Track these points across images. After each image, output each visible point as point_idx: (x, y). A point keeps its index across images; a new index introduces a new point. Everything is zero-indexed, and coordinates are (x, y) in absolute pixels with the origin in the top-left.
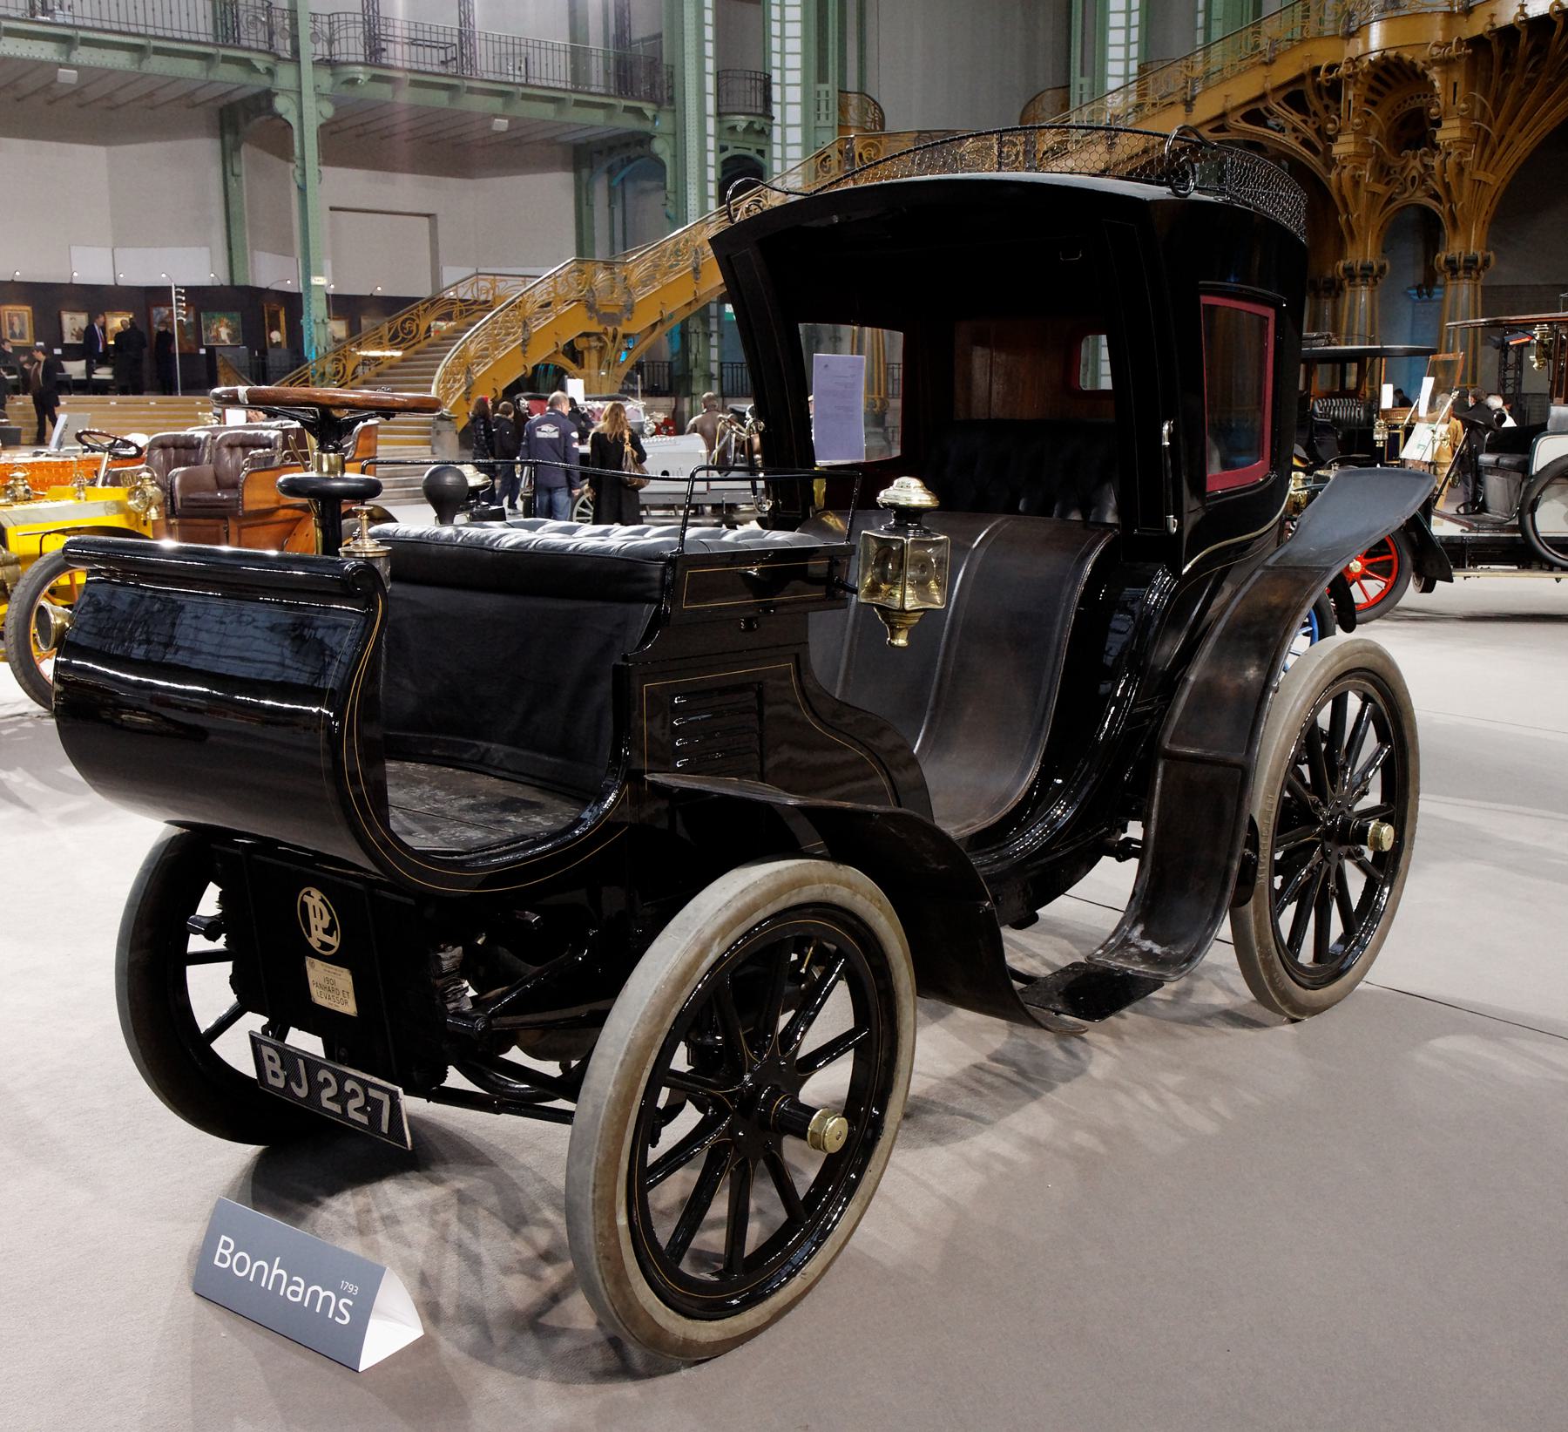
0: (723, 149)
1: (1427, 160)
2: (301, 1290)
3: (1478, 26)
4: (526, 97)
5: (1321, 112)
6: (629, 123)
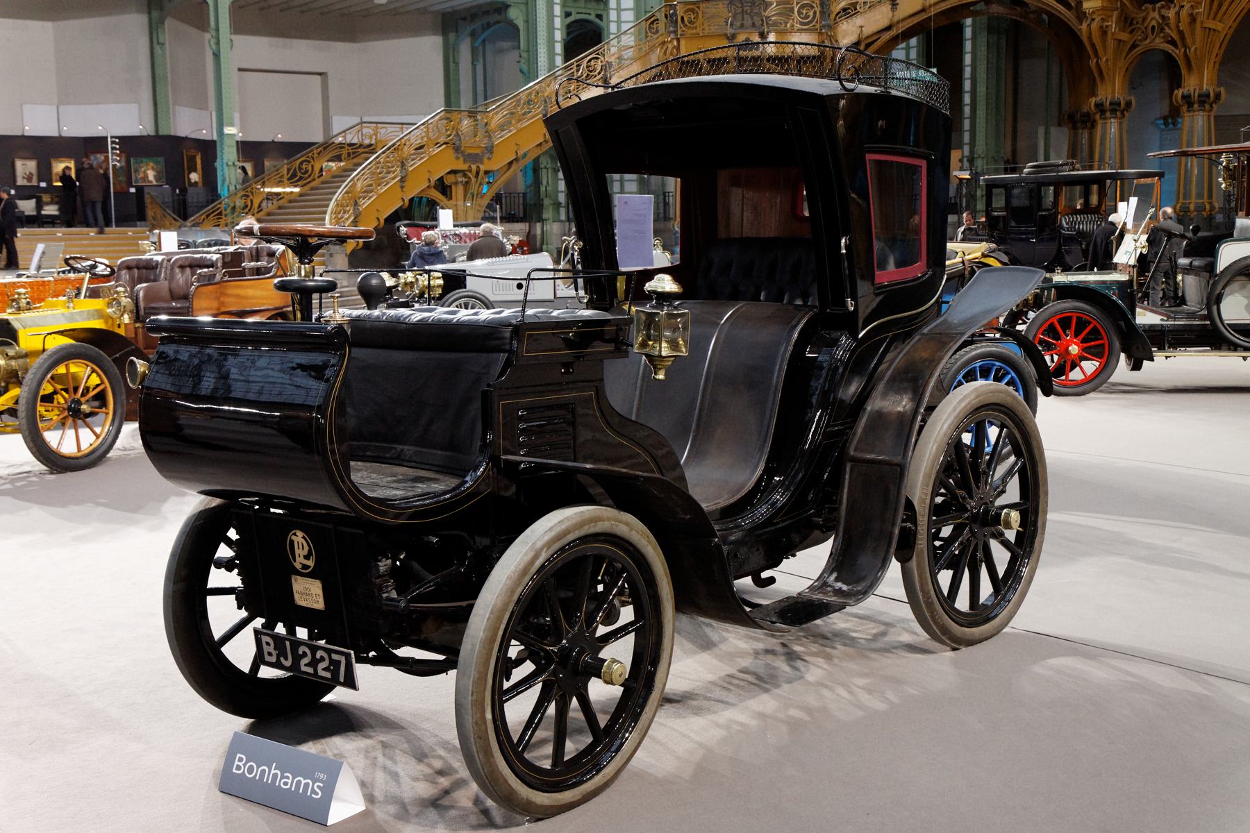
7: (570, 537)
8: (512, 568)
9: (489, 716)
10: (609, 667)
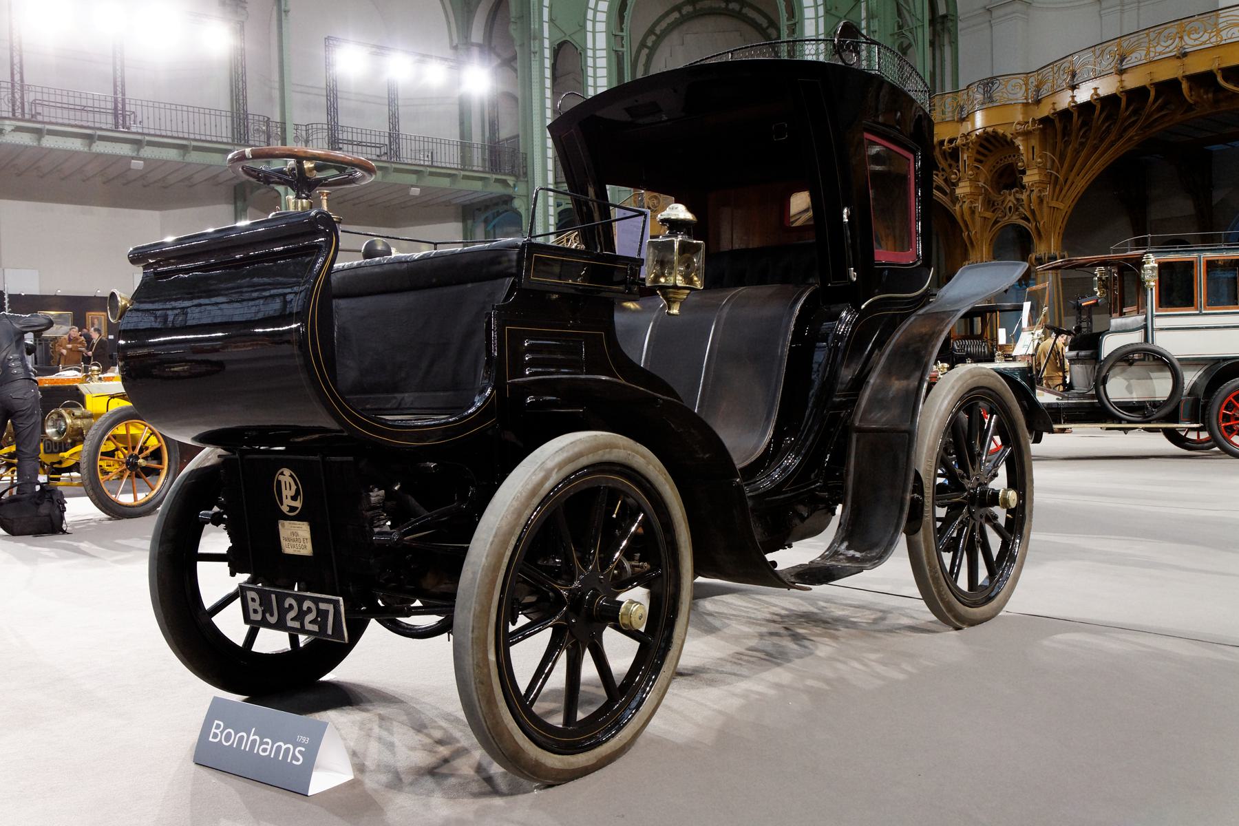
0: (559, 205)
1: (1018, 196)
2: (269, 747)
3: (1045, 111)
4: (431, 174)
5: (948, 169)
6: (498, 190)
7: (584, 461)
9: (492, 657)
10: (627, 609)
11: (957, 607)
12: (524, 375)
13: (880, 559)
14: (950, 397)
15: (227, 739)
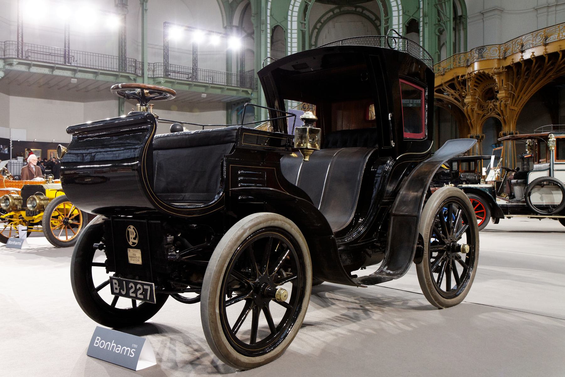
1: (495, 103)
3: (508, 63)
4: (212, 87)
6: (244, 95)
7: (262, 226)
8: (232, 236)
9: (217, 311)
10: (279, 292)
11: (439, 299)
12: (238, 187)
13: (401, 274)
14: (438, 201)
15: (102, 344)
